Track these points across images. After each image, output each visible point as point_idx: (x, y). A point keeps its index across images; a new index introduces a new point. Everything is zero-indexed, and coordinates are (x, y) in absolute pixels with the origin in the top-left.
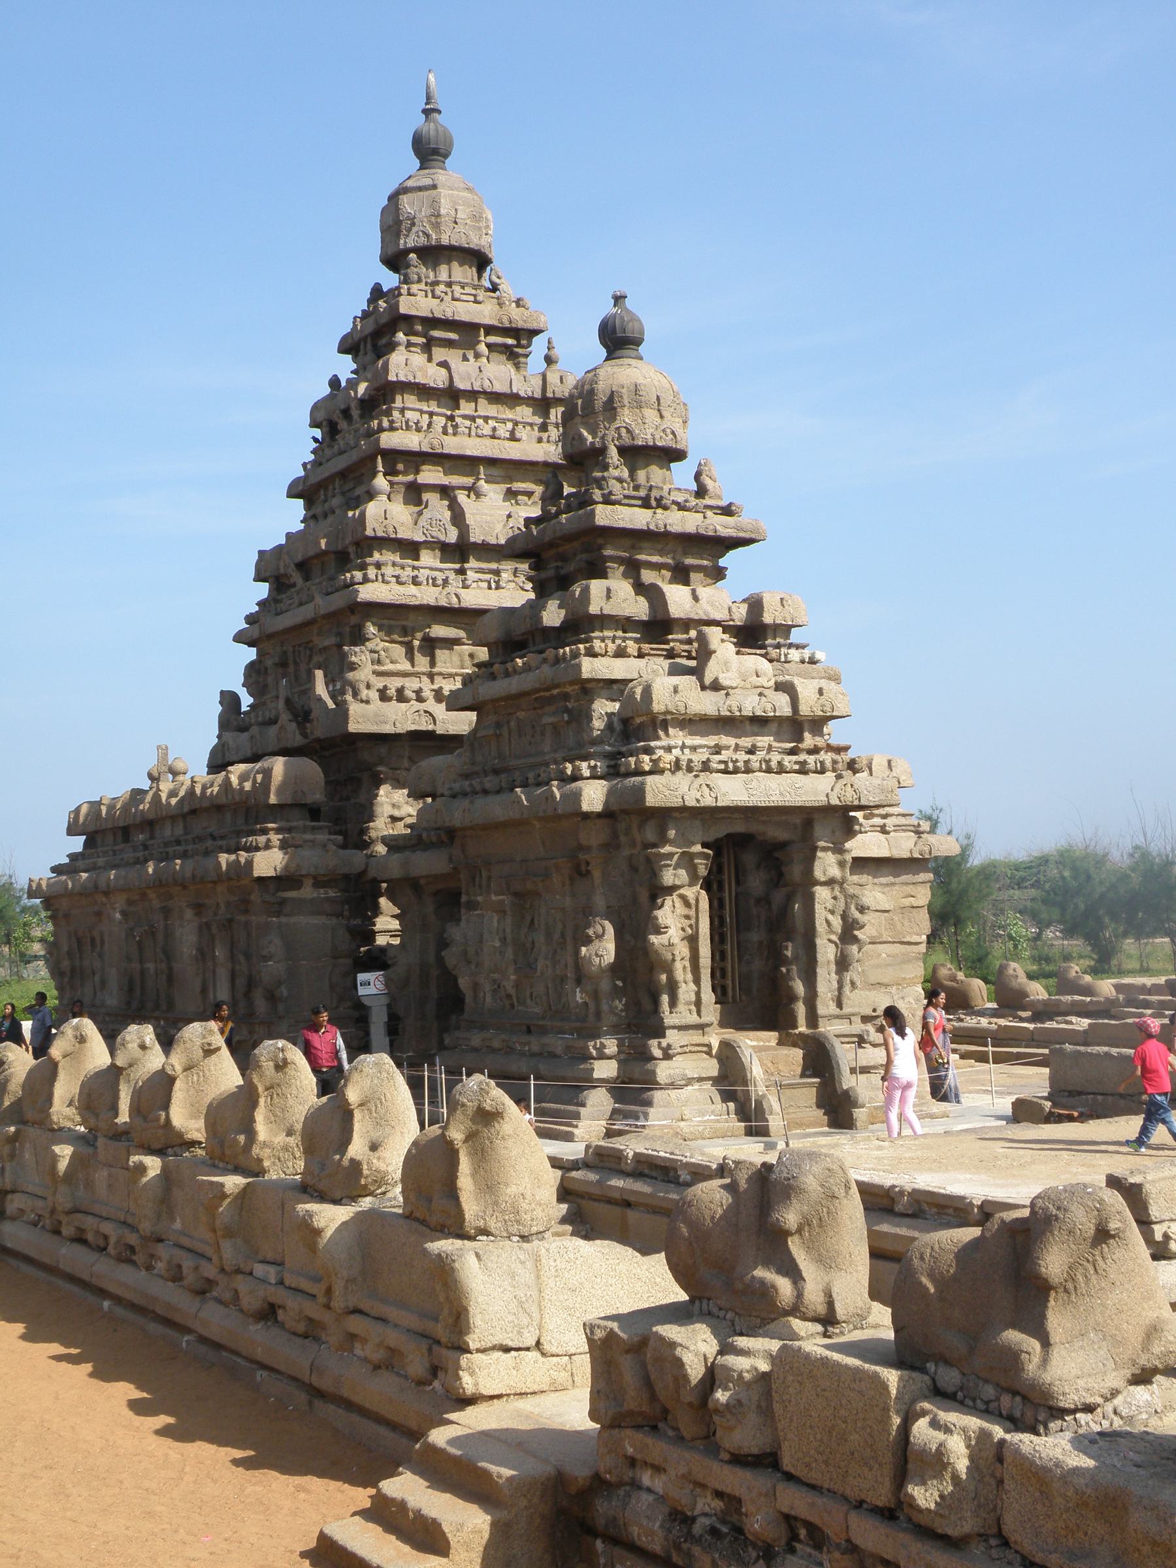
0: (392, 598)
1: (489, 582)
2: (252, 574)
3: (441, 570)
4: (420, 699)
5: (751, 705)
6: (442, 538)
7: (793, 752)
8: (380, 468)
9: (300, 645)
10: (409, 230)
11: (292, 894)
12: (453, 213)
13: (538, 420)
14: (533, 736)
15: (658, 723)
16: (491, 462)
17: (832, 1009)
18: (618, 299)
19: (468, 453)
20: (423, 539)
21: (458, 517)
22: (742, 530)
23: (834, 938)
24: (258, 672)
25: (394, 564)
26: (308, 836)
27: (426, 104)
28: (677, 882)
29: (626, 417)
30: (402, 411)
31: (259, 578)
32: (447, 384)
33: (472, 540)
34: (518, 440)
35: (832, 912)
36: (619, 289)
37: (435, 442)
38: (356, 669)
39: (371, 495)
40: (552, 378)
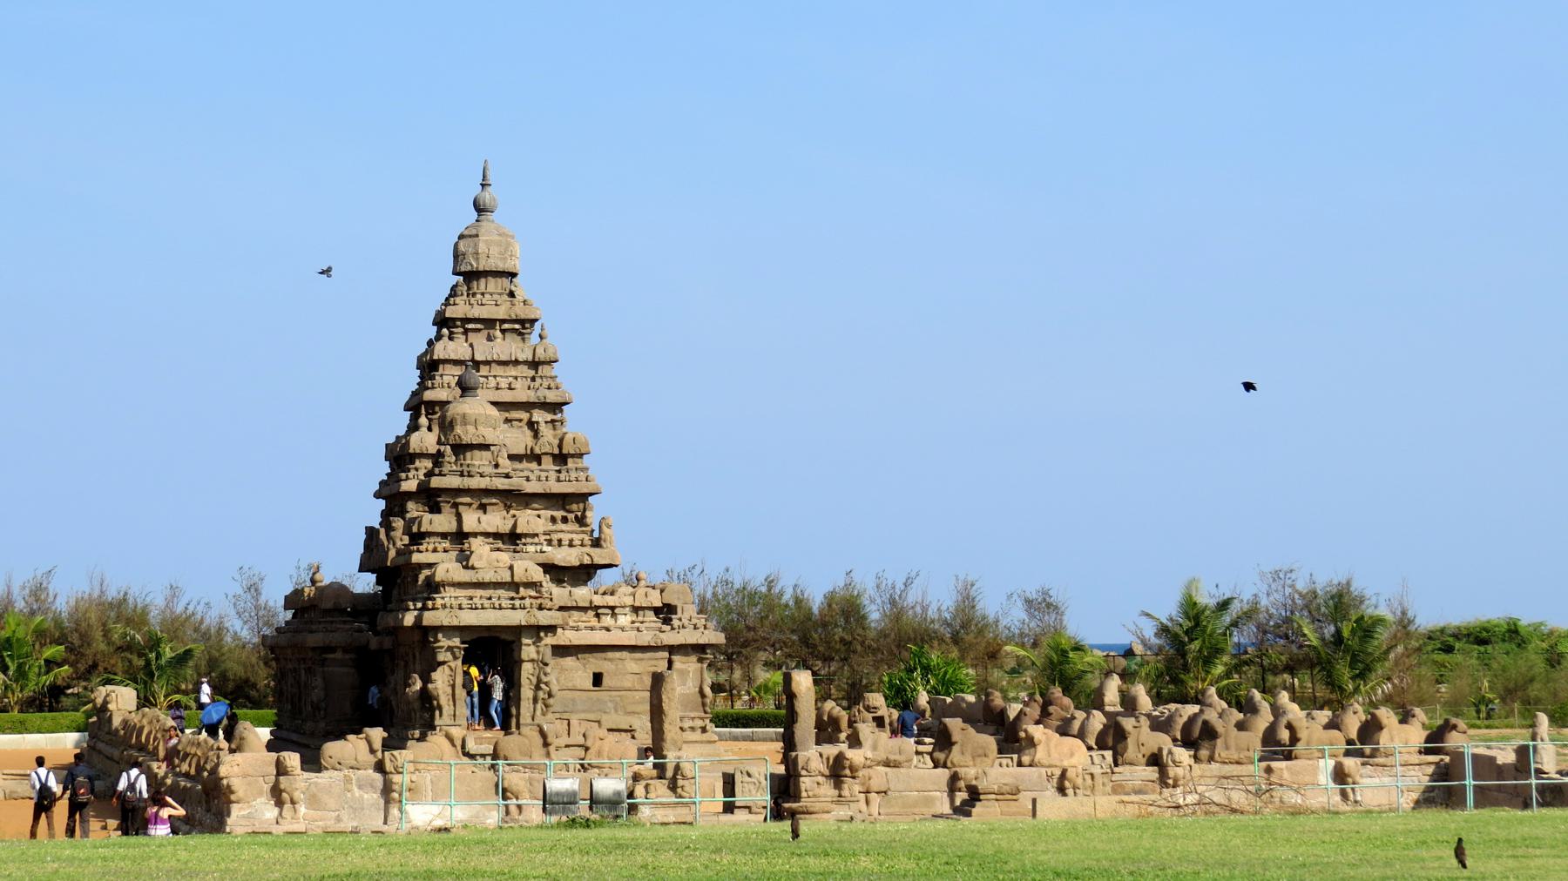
5: (488, 576)
7: (512, 599)
8: (423, 412)
10: (462, 261)
11: (332, 656)
13: (532, 373)
17: (529, 720)
22: (514, 486)
23: (533, 687)
26: (342, 626)
28: (446, 660)
29: (458, 430)
31: (386, 460)
32: (471, 357)
35: (533, 675)
38: (394, 530)
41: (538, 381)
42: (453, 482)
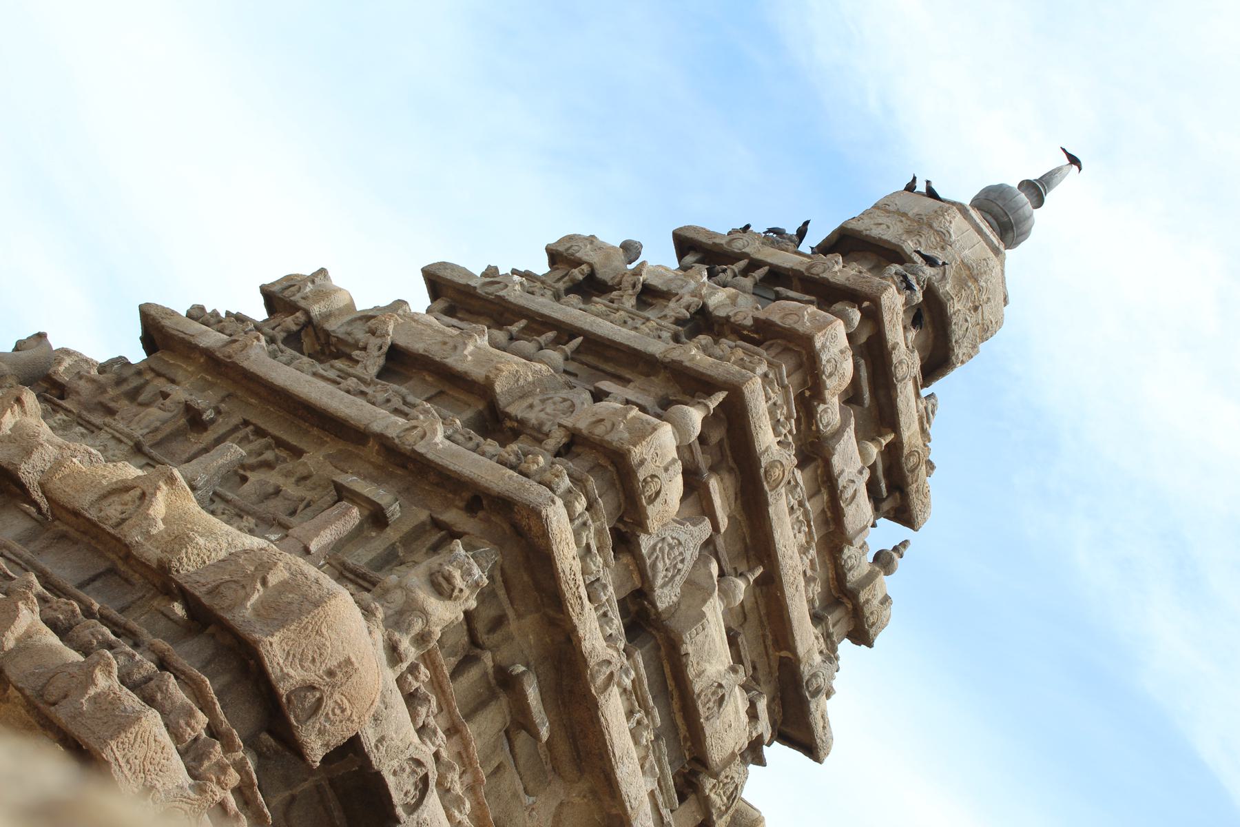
0: (567, 572)
2: (272, 276)
6: (659, 582)
9: (259, 432)
12: (985, 297)
20: (645, 550)
21: (696, 589)
24: (120, 381)
25: (599, 533)
27: (1035, 180)
33: (686, 637)
37: (777, 472)
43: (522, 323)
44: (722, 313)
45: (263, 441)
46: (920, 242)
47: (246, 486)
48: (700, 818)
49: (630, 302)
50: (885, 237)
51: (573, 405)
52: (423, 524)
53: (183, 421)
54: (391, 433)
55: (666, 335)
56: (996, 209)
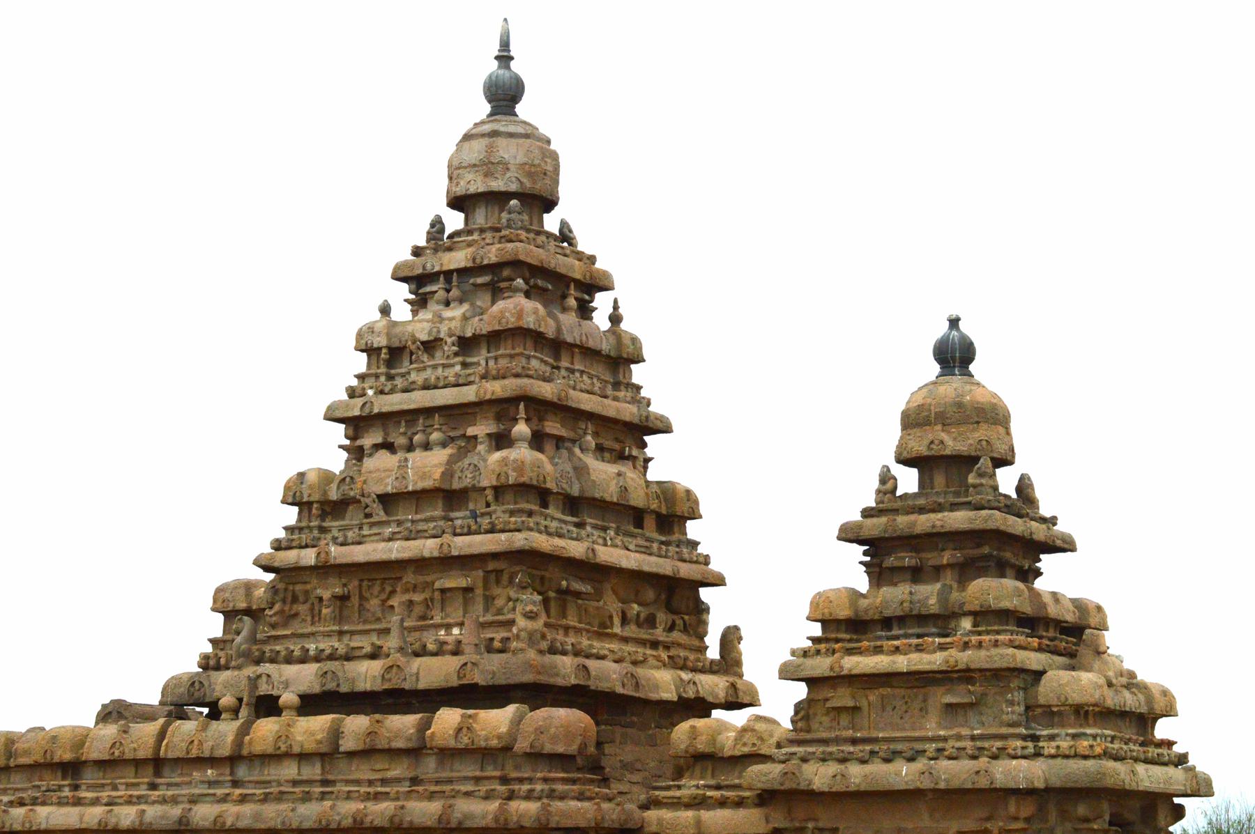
1: (605, 539)
3: (565, 522)
4: (564, 653)
6: (569, 490)
8: (522, 414)
14: (906, 712)
15: (1082, 713)
16: (591, 416)
18: (954, 323)
19: (583, 407)
21: (581, 471)
24: (284, 601)
25: (542, 514)
27: (499, 51)
30: (528, 358)
34: (606, 397)
36: (954, 313)
37: (563, 394)
39: (501, 440)
40: (627, 341)
41: (622, 388)
42: (1016, 525)
43: (403, 424)
44: (469, 334)
45: (378, 582)
46: (496, 178)
47: (396, 609)
48: (654, 516)
49: (425, 358)
50: (479, 191)
51: (475, 466)
52: (484, 576)
53: (338, 603)
54: (436, 554)
55: (458, 368)
56: (501, 97)
